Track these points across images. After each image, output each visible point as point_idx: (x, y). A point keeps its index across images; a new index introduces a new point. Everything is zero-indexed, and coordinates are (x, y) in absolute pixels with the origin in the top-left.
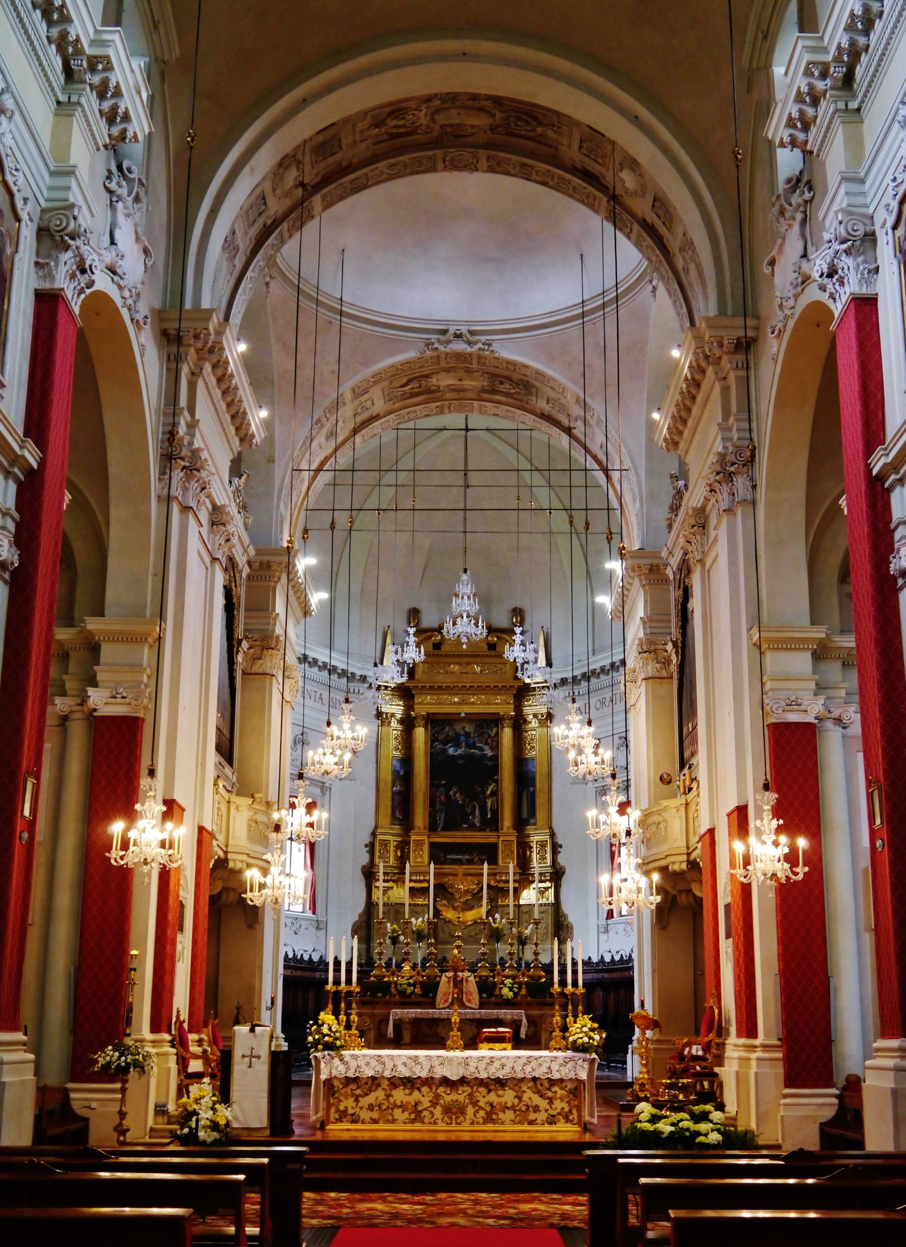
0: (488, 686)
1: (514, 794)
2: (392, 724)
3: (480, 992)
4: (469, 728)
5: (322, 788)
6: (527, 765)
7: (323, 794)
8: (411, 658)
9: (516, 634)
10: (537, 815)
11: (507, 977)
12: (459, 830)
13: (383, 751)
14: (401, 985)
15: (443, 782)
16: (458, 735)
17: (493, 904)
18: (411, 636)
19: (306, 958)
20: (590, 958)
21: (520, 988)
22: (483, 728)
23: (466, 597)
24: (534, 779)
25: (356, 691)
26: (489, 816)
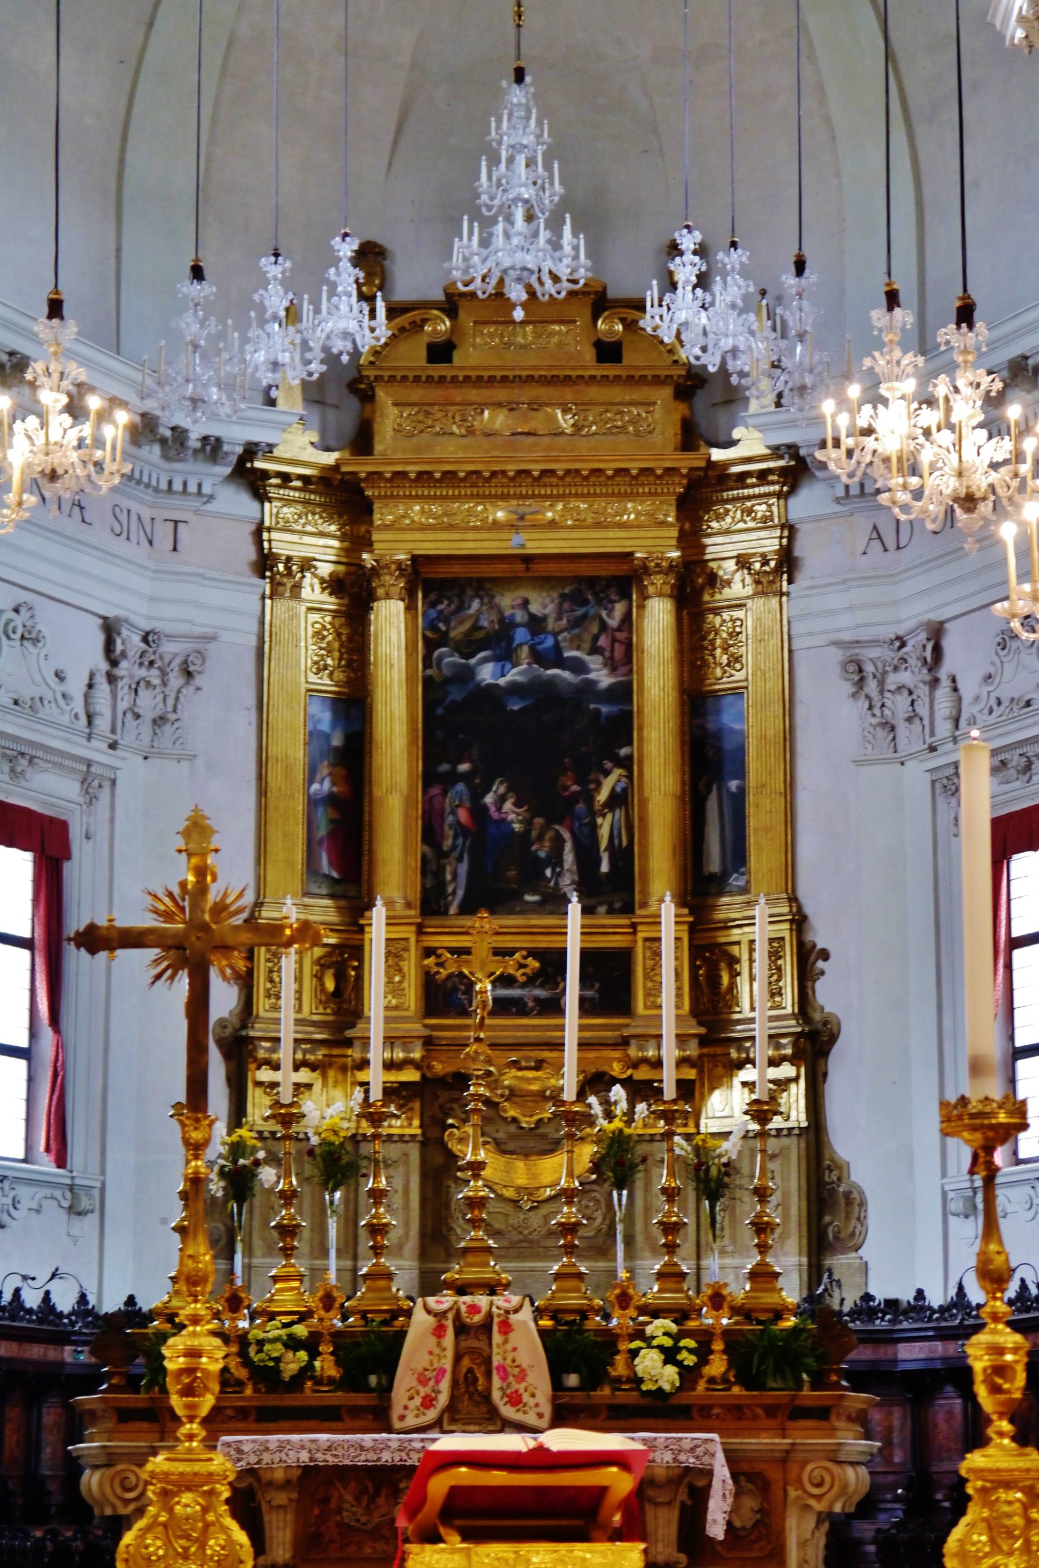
0: (595, 472)
1: (681, 799)
2: (306, 593)
3: (557, 1371)
4: (542, 604)
5: (84, 781)
6: (718, 712)
7: (91, 799)
8: (346, 335)
9: (681, 253)
10: (753, 860)
11: (656, 1313)
12: (510, 912)
13: (274, 670)
14: (261, 1343)
15: (464, 767)
16: (507, 626)
18: (346, 265)
19: (32, 1299)
20: (920, 1294)
21: (703, 1353)
22: (585, 602)
23: (521, 160)
24: (741, 751)
25: (192, 488)
26: (605, 867)
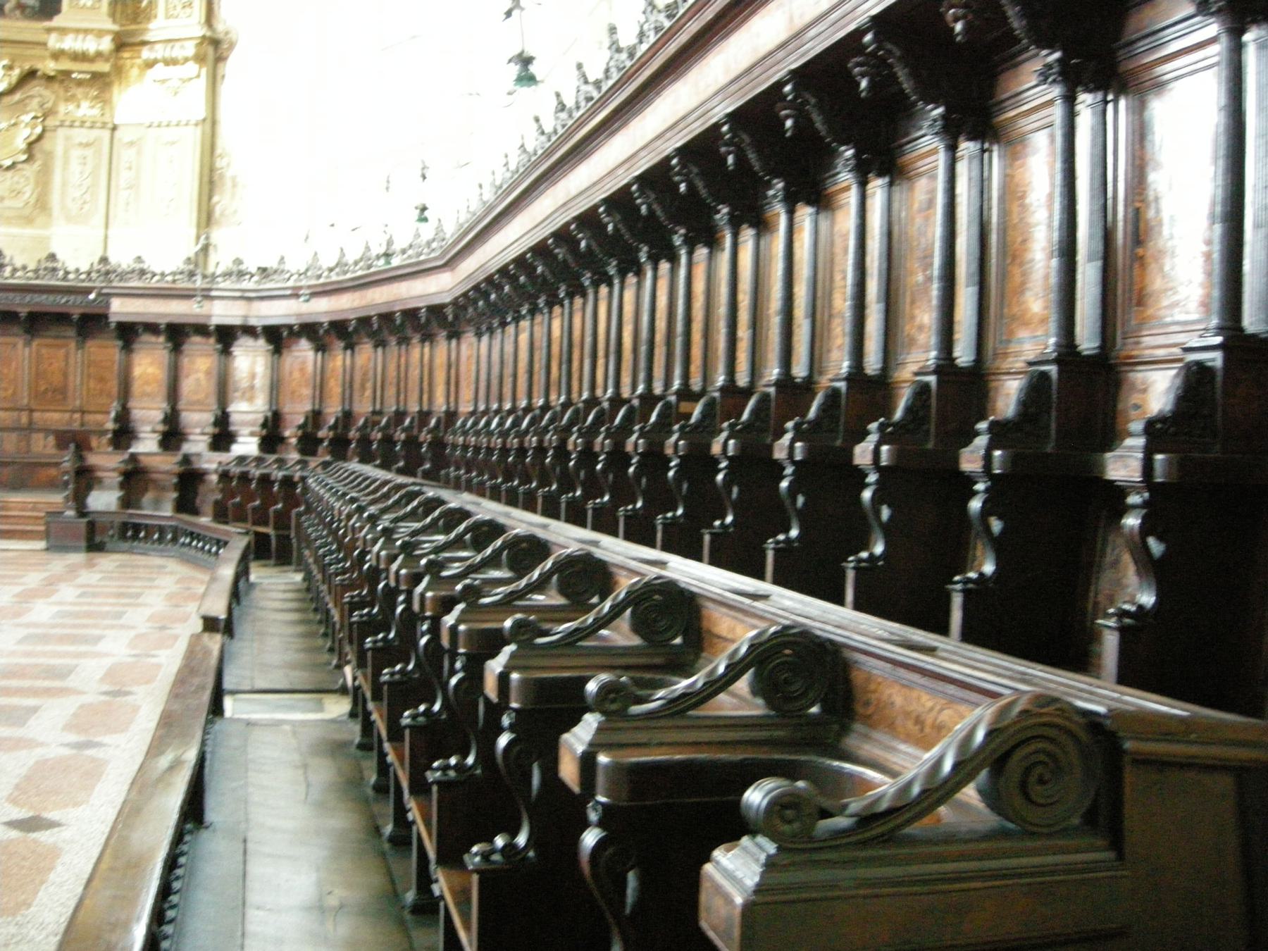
17: (50, 122)
